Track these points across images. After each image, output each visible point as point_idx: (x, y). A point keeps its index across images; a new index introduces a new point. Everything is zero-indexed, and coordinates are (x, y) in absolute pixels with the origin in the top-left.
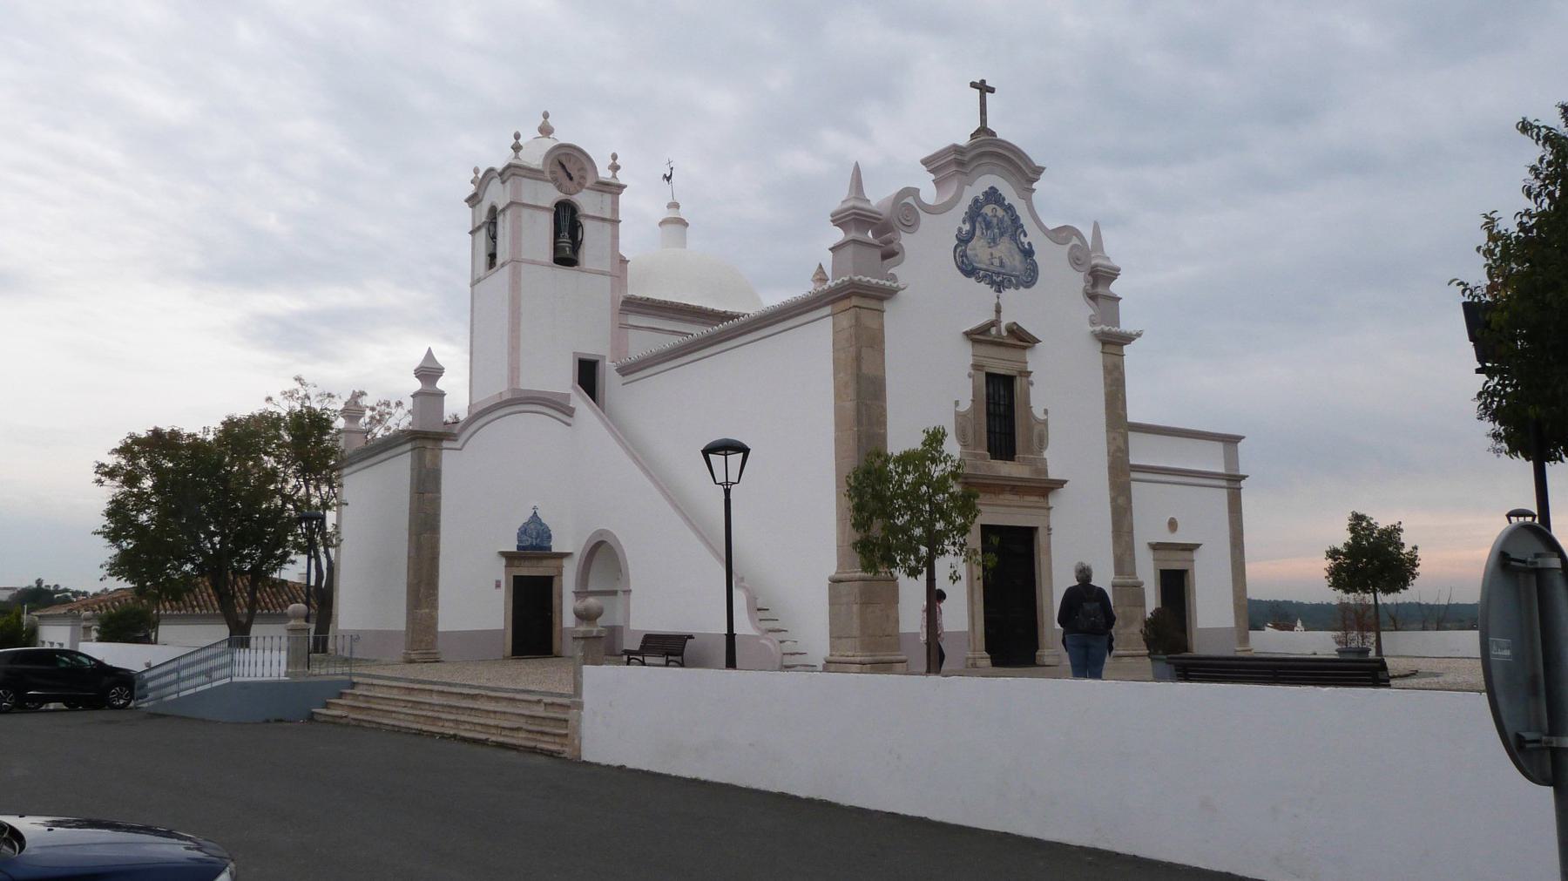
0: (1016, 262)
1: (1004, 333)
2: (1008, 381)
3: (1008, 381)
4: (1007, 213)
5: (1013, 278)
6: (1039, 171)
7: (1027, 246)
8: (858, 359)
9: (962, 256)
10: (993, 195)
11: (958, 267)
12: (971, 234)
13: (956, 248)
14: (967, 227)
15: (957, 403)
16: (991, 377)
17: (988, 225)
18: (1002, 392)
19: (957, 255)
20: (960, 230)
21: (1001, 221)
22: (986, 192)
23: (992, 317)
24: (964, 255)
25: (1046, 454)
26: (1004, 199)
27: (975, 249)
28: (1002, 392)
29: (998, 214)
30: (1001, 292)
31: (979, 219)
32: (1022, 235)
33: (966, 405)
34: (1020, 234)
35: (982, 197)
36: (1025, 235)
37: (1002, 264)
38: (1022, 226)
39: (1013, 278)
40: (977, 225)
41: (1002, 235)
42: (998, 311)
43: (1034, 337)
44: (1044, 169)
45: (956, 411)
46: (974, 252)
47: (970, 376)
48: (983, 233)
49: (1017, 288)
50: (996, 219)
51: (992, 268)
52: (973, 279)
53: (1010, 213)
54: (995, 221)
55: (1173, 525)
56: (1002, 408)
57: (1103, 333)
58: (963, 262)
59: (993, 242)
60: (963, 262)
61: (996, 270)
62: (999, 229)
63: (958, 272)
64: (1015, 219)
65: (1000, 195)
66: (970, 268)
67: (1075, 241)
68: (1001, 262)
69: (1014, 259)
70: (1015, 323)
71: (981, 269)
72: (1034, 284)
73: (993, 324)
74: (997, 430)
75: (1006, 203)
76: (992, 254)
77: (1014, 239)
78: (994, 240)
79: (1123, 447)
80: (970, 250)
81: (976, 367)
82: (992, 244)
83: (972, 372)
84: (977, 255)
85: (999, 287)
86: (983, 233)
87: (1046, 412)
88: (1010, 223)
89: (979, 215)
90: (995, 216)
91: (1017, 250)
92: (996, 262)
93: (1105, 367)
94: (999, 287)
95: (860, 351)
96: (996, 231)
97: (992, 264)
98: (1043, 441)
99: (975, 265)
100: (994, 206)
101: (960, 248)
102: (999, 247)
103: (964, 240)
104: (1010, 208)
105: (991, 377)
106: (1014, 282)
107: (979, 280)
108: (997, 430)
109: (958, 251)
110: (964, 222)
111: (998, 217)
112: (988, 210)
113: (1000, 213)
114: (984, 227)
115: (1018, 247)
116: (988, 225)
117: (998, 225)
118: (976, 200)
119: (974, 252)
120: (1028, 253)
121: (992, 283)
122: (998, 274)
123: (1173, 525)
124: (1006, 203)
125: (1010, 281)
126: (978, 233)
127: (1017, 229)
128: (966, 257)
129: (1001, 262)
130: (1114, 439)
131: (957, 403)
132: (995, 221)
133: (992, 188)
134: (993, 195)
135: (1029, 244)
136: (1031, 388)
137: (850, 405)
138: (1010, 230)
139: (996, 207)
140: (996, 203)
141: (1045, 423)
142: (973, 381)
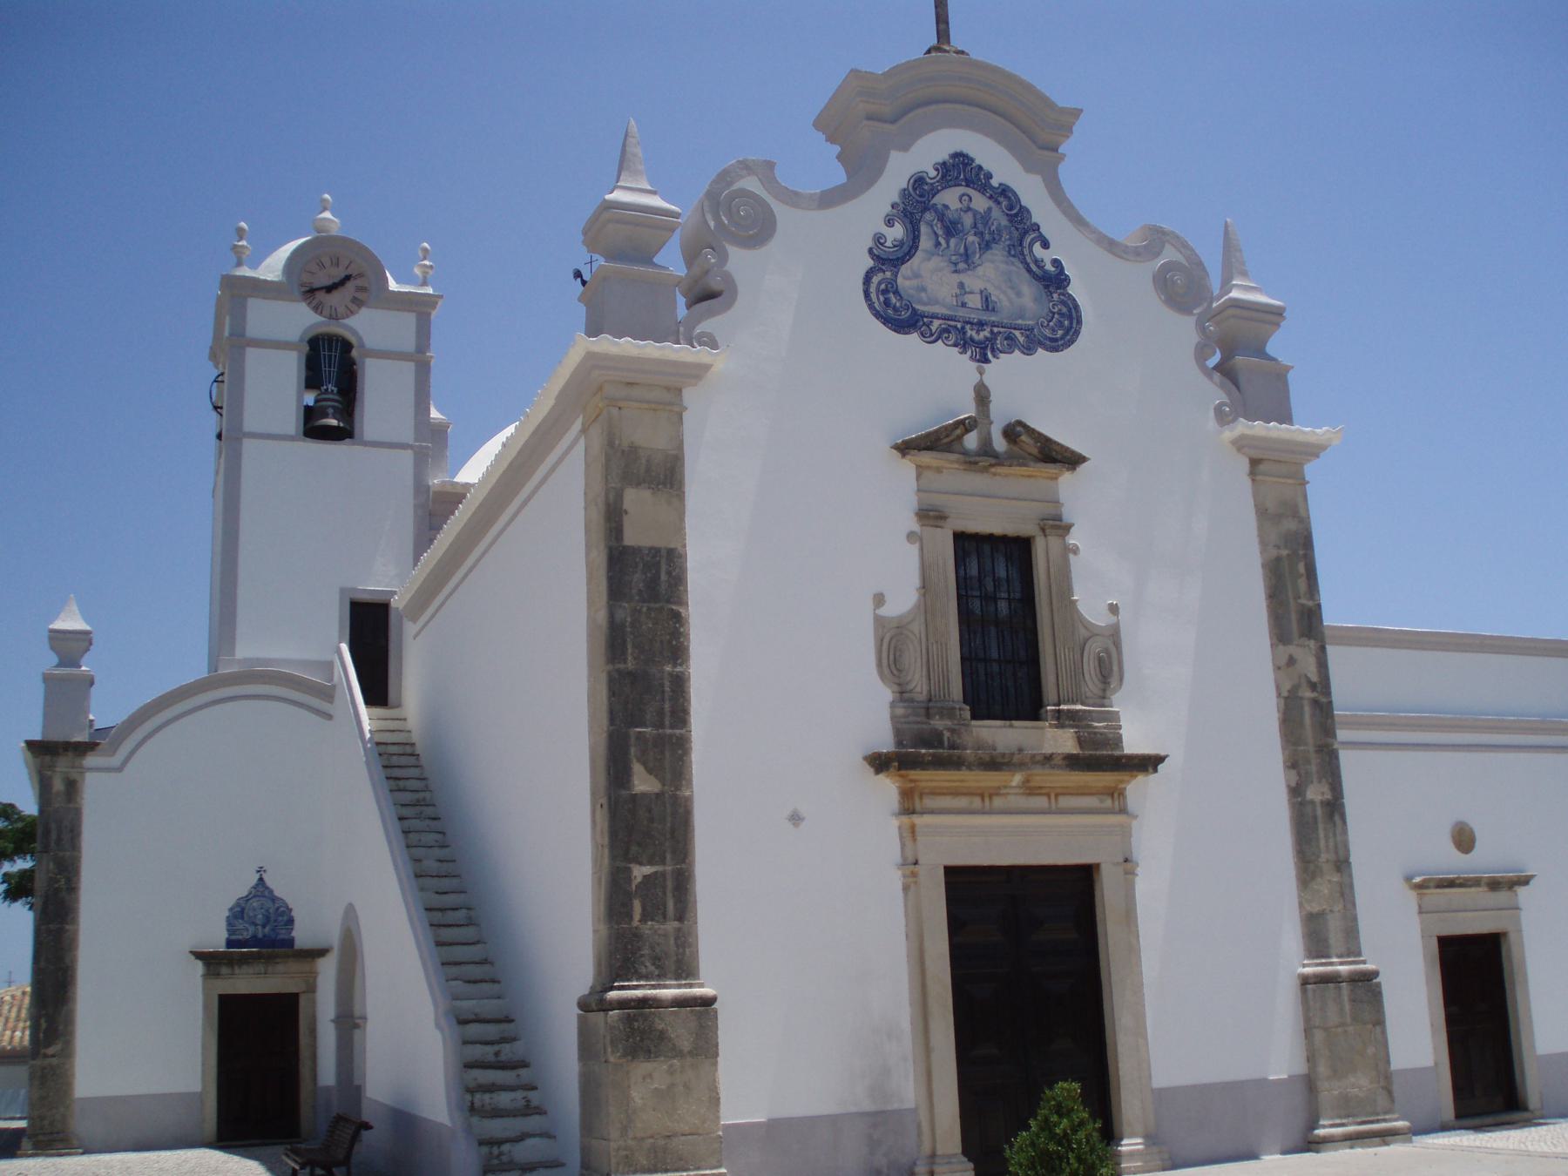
0: (1024, 300)
1: (1000, 444)
2: (1018, 549)
3: (1018, 549)
4: (999, 203)
5: (1017, 333)
6: (1065, 120)
7: (1049, 267)
8: (613, 518)
9: (885, 292)
10: (960, 169)
11: (877, 315)
12: (909, 249)
13: (867, 280)
14: (897, 232)
15: (879, 600)
16: (964, 541)
17: (951, 228)
18: (1002, 573)
19: (873, 289)
20: (879, 239)
21: (986, 217)
22: (944, 163)
23: (968, 411)
24: (890, 288)
25: (1120, 703)
26: (989, 176)
27: (916, 276)
28: (1002, 573)
29: (973, 205)
30: (987, 361)
31: (928, 216)
32: (1037, 247)
33: (903, 599)
34: (1031, 245)
35: (933, 173)
36: (1046, 245)
37: (988, 304)
38: (1036, 227)
39: (1017, 333)
40: (924, 229)
41: (986, 246)
42: (982, 396)
43: (1073, 452)
44: (1081, 110)
45: (879, 622)
46: (915, 283)
47: (911, 536)
48: (938, 244)
49: (1028, 350)
50: (970, 214)
51: (961, 313)
52: (914, 338)
53: (1004, 203)
54: (968, 220)
55: (1464, 840)
56: (1003, 606)
57: (1242, 437)
58: (887, 303)
59: (967, 258)
60: (887, 303)
61: (975, 317)
62: (980, 234)
63: (877, 325)
64: (1019, 217)
65: (980, 168)
66: (905, 315)
67: (1169, 254)
68: (986, 299)
69: (1019, 294)
70: (1020, 423)
71: (934, 316)
72: (1072, 342)
73: (966, 426)
74: (995, 655)
75: (995, 182)
76: (961, 285)
77: (1017, 250)
78: (966, 256)
79: (1315, 679)
80: (906, 278)
81: (930, 515)
82: (962, 266)
83: (916, 527)
84: (923, 289)
85: (983, 353)
86: (938, 244)
87: (1114, 609)
88: (1004, 222)
89: (926, 209)
90: (969, 209)
91: (1027, 275)
92: (975, 301)
93: (1262, 512)
94: (983, 353)
95: (620, 496)
96: (971, 238)
97: (964, 305)
98: (1108, 671)
99: (917, 307)
100: (961, 190)
101: (880, 276)
102: (980, 270)
103: (887, 260)
104: (1005, 192)
105: (964, 541)
106: (1021, 339)
107: (931, 337)
108: (995, 655)
109: (875, 280)
110: (889, 222)
111: (975, 213)
112: (950, 198)
113: (980, 203)
114: (940, 232)
115: (1029, 270)
116: (951, 228)
117: (975, 226)
118: (919, 181)
119: (915, 283)
120: (1054, 281)
121: (964, 344)
122: (981, 325)
123: (1464, 840)
124: (995, 182)
125: (1010, 338)
126: (925, 242)
127: (1026, 232)
128: (896, 292)
129: (986, 299)
130: (1291, 661)
131: (879, 600)
132: (968, 220)
133: (956, 155)
134: (960, 169)
135: (1056, 263)
136: (1071, 556)
137: (602, 616)
138: (1005, 236)
139: (970, 191)
140: (968, 183)
141: (1114, 634)
142: (921, 549)
